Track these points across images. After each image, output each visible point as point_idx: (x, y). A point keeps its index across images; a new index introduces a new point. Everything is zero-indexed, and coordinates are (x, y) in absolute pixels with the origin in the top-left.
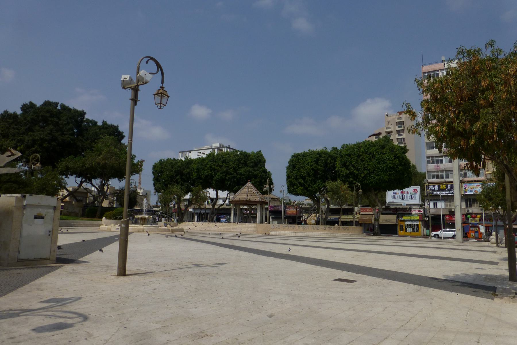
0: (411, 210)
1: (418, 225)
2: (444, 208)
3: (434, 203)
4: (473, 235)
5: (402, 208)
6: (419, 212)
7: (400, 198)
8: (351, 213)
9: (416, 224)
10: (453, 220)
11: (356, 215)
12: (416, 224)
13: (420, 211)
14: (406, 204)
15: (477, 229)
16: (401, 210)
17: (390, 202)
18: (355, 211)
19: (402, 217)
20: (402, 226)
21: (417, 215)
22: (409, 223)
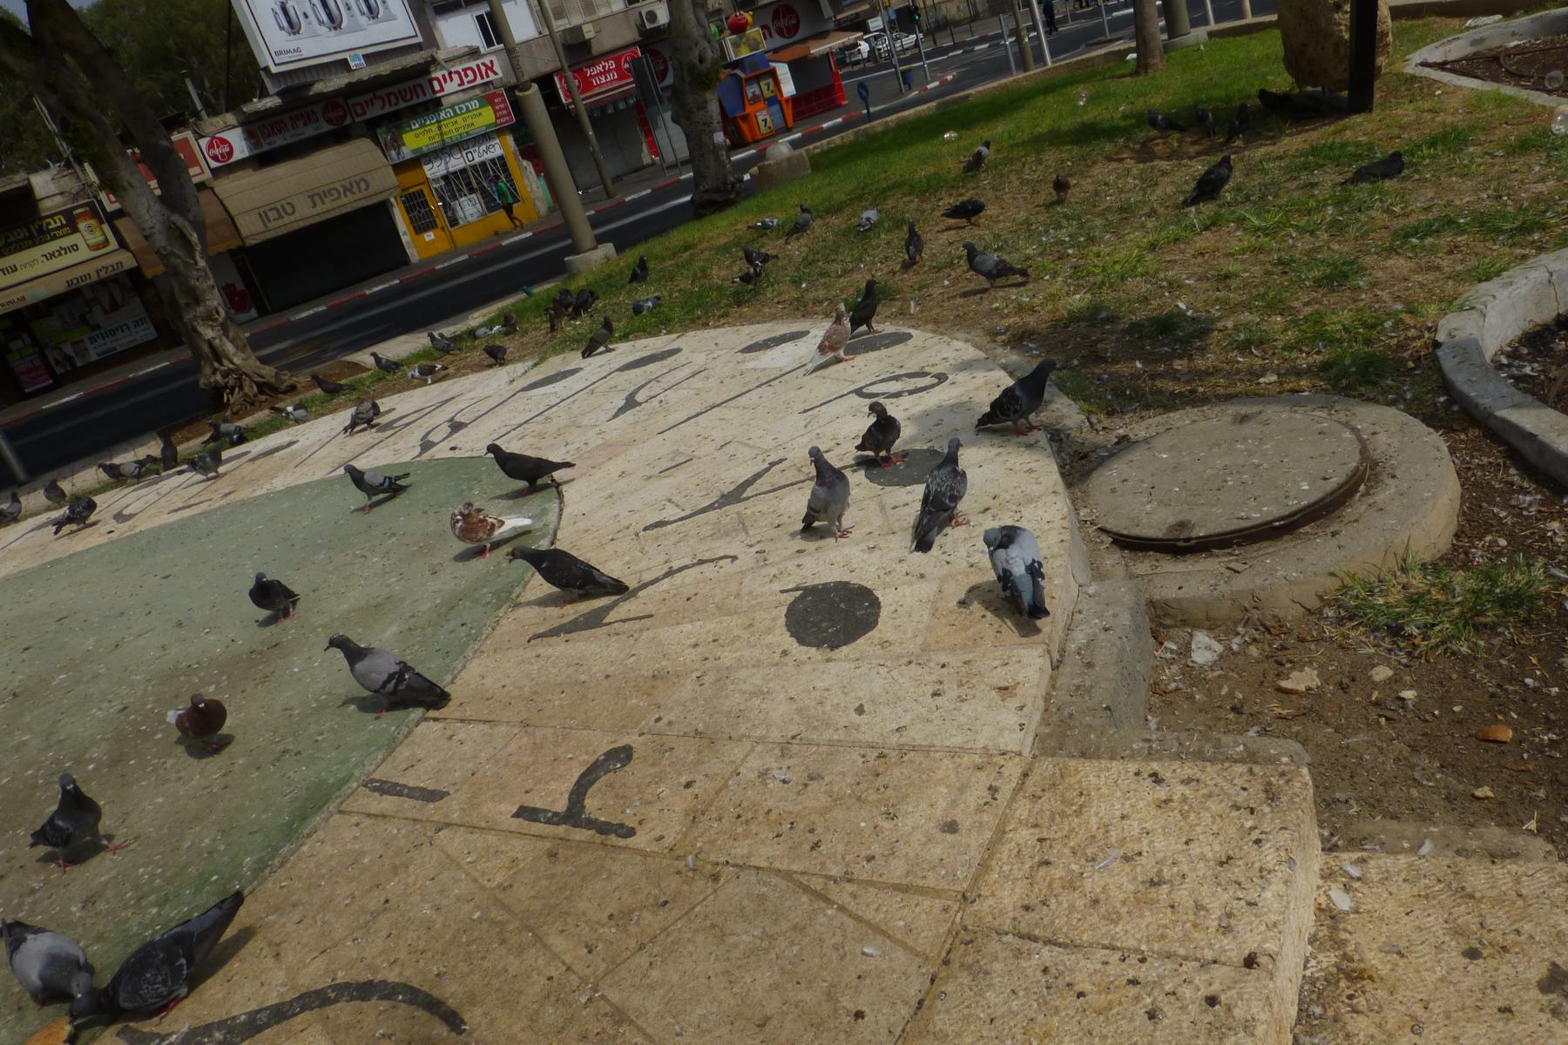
0: (431, 81)
1: (501, 158)
2: (537, 35)
3: (480, 19)
4: (765, 120)
5: (394, 72)
6: (479, 81)
7: (321, 23)
8: (23, 233)
9: (492, 161)
10: (597, 90)
11: (75, 230)
12: (490, 156)
13: (483, 69)
14: (365, 56)
15: (768, 85)
16: (368, 96)
17: (285, 58)
18: (47, 204)
19: (397, 143)
20: (415, 203)
21: (476, 97)
22: (456, 162)
